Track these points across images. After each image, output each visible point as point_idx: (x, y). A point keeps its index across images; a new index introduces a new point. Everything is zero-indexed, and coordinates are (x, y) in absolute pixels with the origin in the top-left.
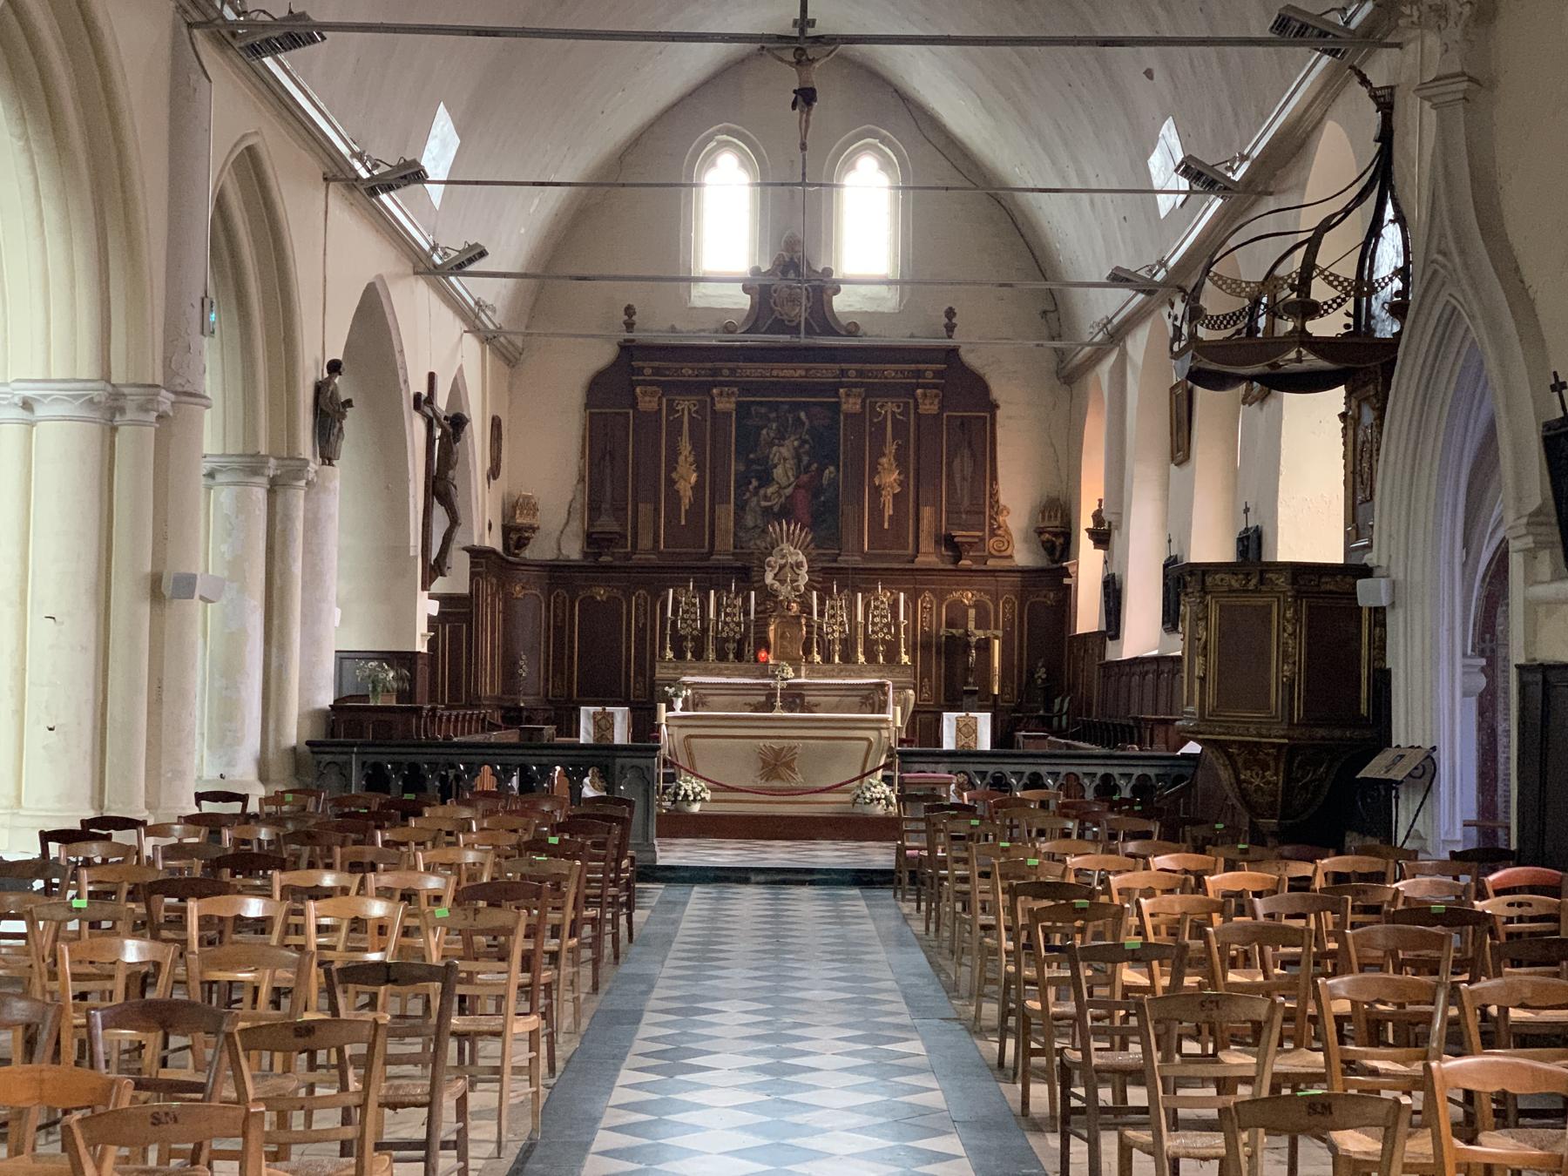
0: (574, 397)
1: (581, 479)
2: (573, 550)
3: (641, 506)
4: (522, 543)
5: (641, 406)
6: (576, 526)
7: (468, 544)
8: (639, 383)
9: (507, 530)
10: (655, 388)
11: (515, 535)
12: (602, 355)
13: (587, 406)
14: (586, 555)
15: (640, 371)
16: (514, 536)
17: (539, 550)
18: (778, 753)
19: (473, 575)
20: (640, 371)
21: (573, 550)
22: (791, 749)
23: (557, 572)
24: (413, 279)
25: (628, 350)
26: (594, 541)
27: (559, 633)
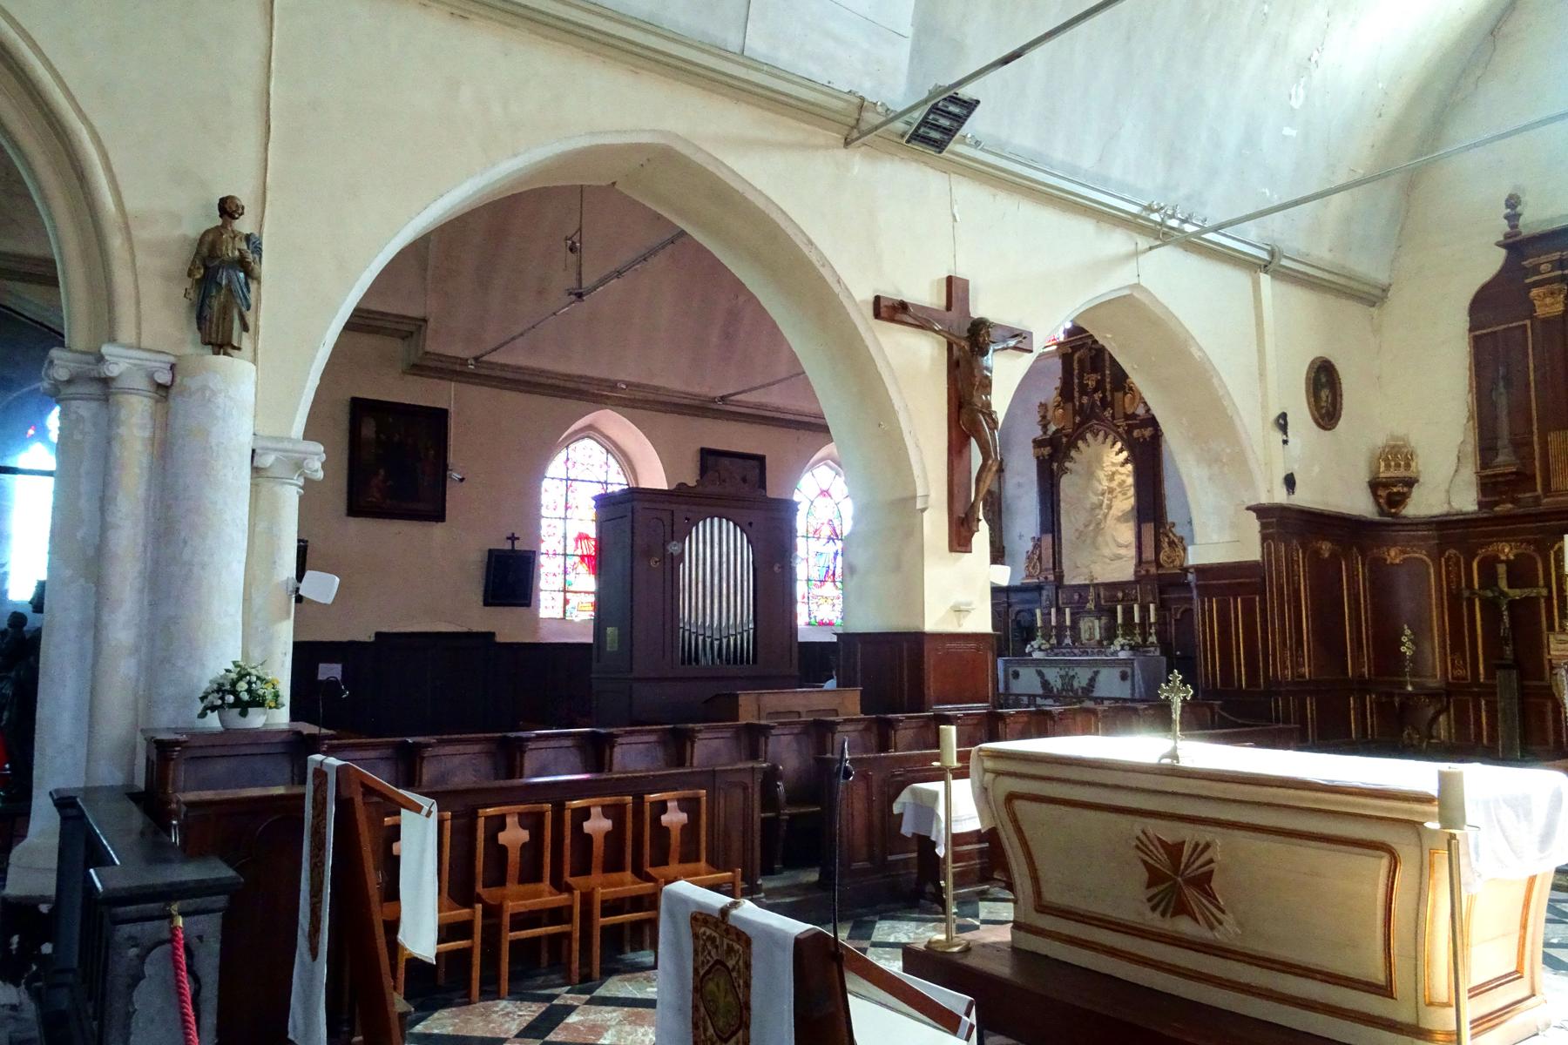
0: (1462, 321)
1: (1471, 417)
2: (1467, 501)
3: (1552, 437)
4: (1397, 500)
5: (1541, 312)
6: (1469, 474)
7: (1253, 503)
8: (1536, 284)
9: (1375, 485)
10: (1556, 286)
11: (1391, 489)
12: (1491, 262)
13: (1471, 330)
14: (1480, 504)
15: (1536, 270)
16: (1383, 493)
17: (1424, 503)
18: (1174, 850)
19: (1264, 538)
20: (1536, 270)
21: (1467, 501)
22: (1202, 848)
23: (1447, 528)
24: (842, 154)
25: (1517, 246)
26: (1489, 486)
27: (1455, 603)
